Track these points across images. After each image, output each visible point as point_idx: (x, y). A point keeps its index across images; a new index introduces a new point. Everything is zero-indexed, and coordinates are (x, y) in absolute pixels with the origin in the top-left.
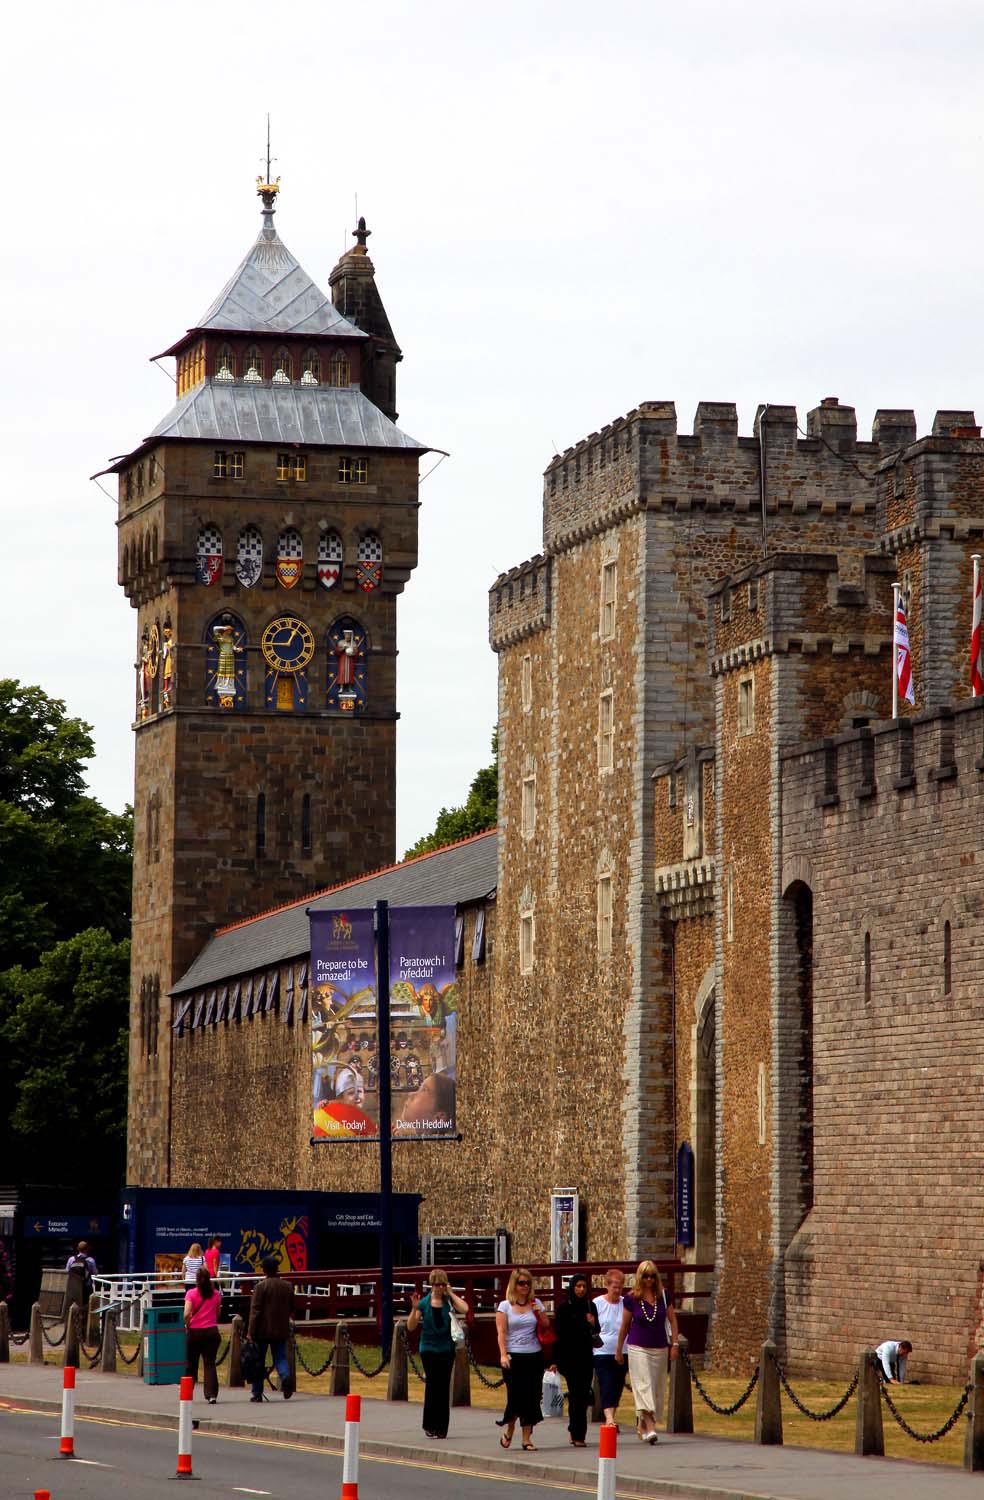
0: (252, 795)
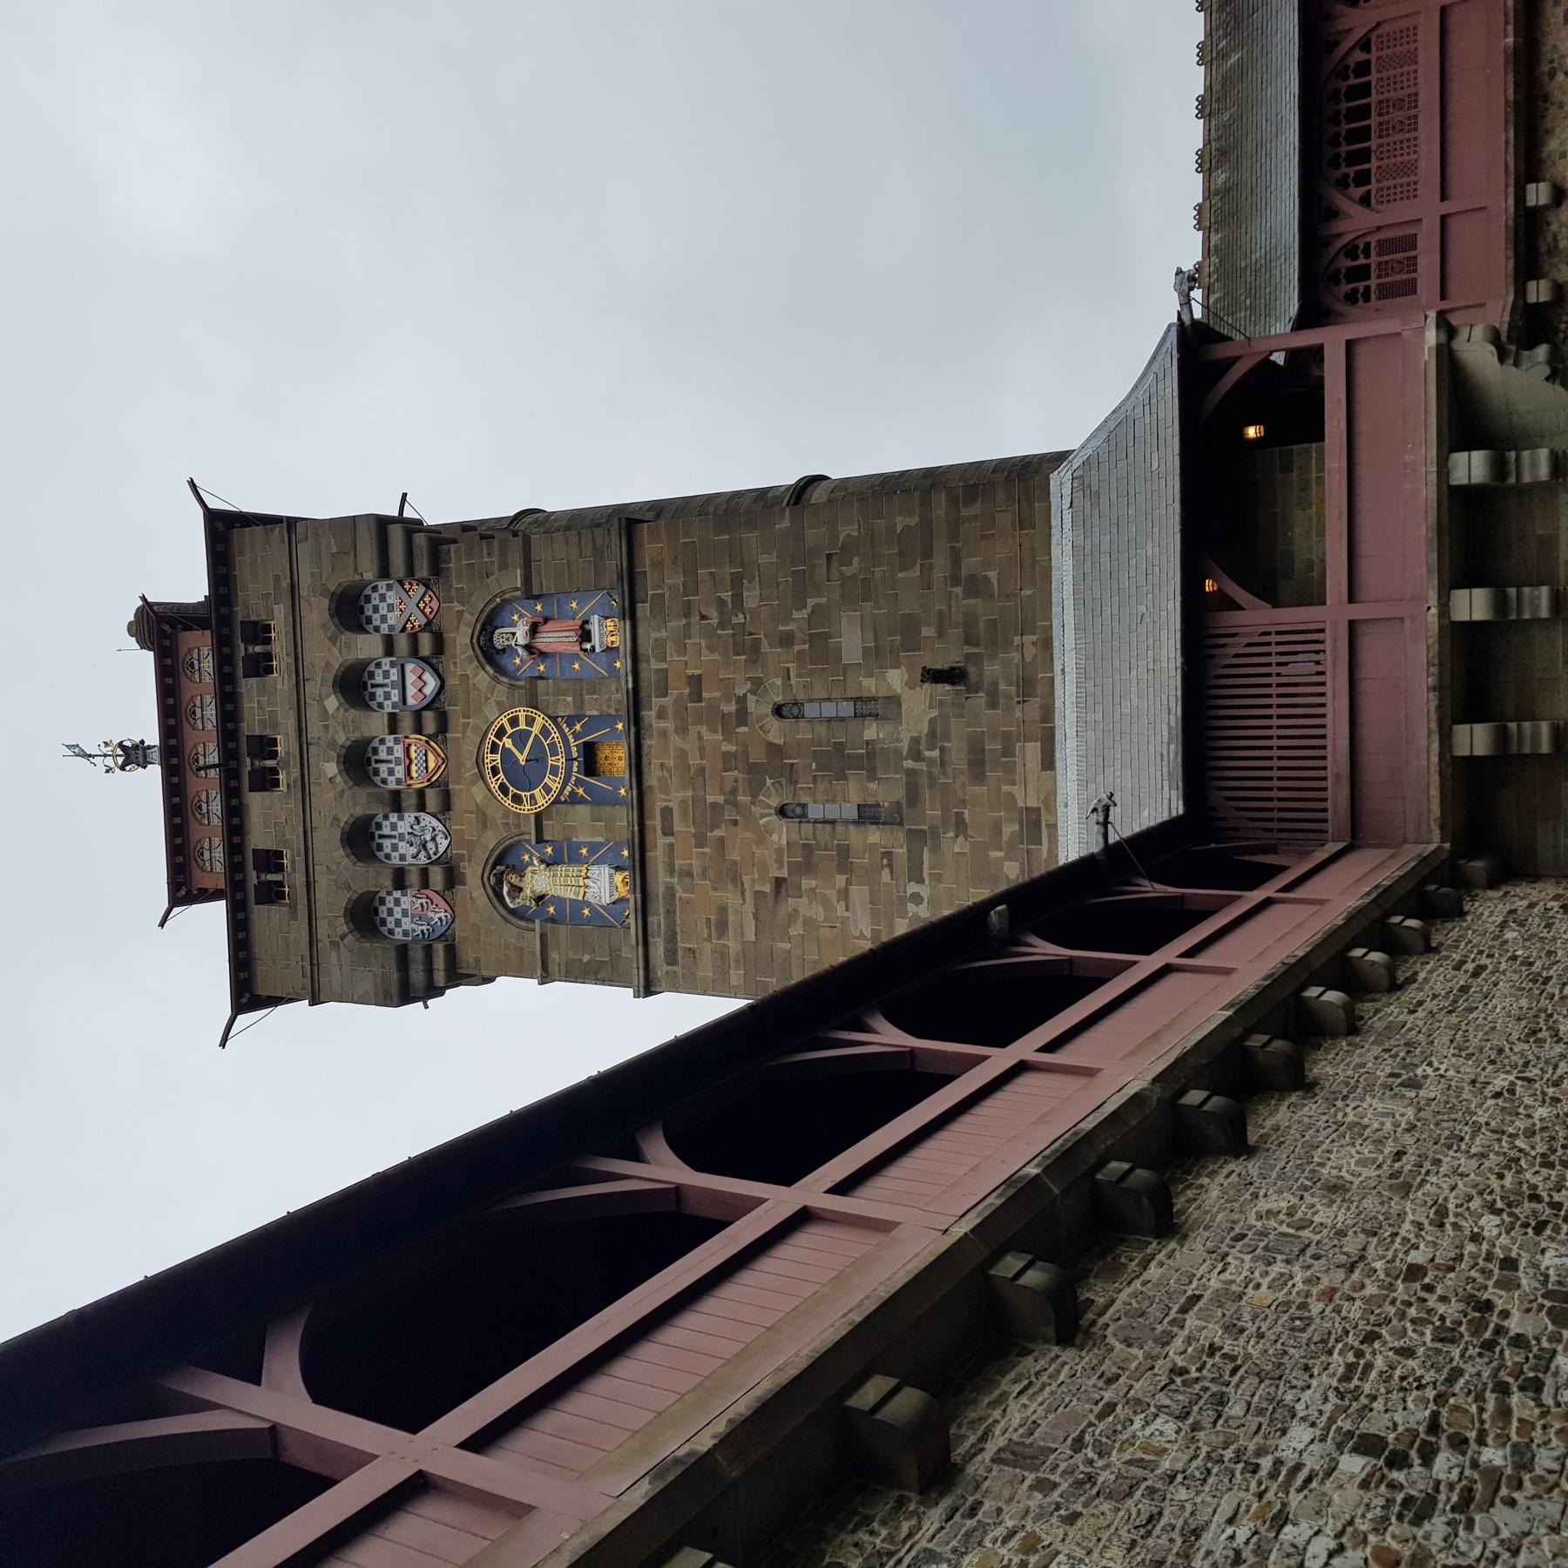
0: (782, 833)
